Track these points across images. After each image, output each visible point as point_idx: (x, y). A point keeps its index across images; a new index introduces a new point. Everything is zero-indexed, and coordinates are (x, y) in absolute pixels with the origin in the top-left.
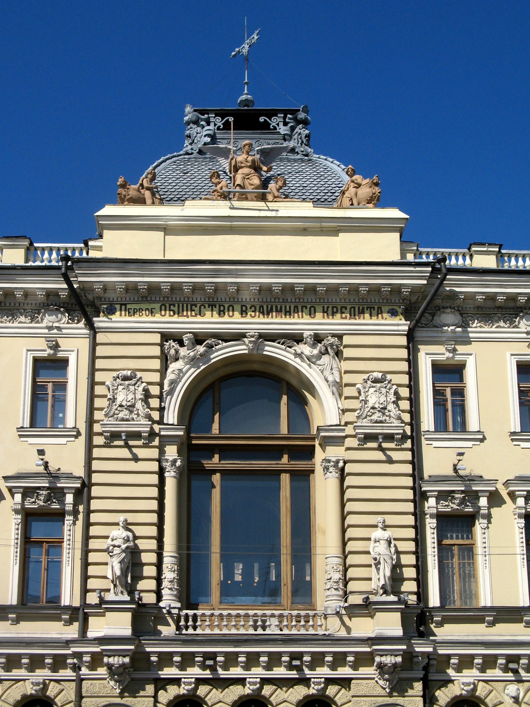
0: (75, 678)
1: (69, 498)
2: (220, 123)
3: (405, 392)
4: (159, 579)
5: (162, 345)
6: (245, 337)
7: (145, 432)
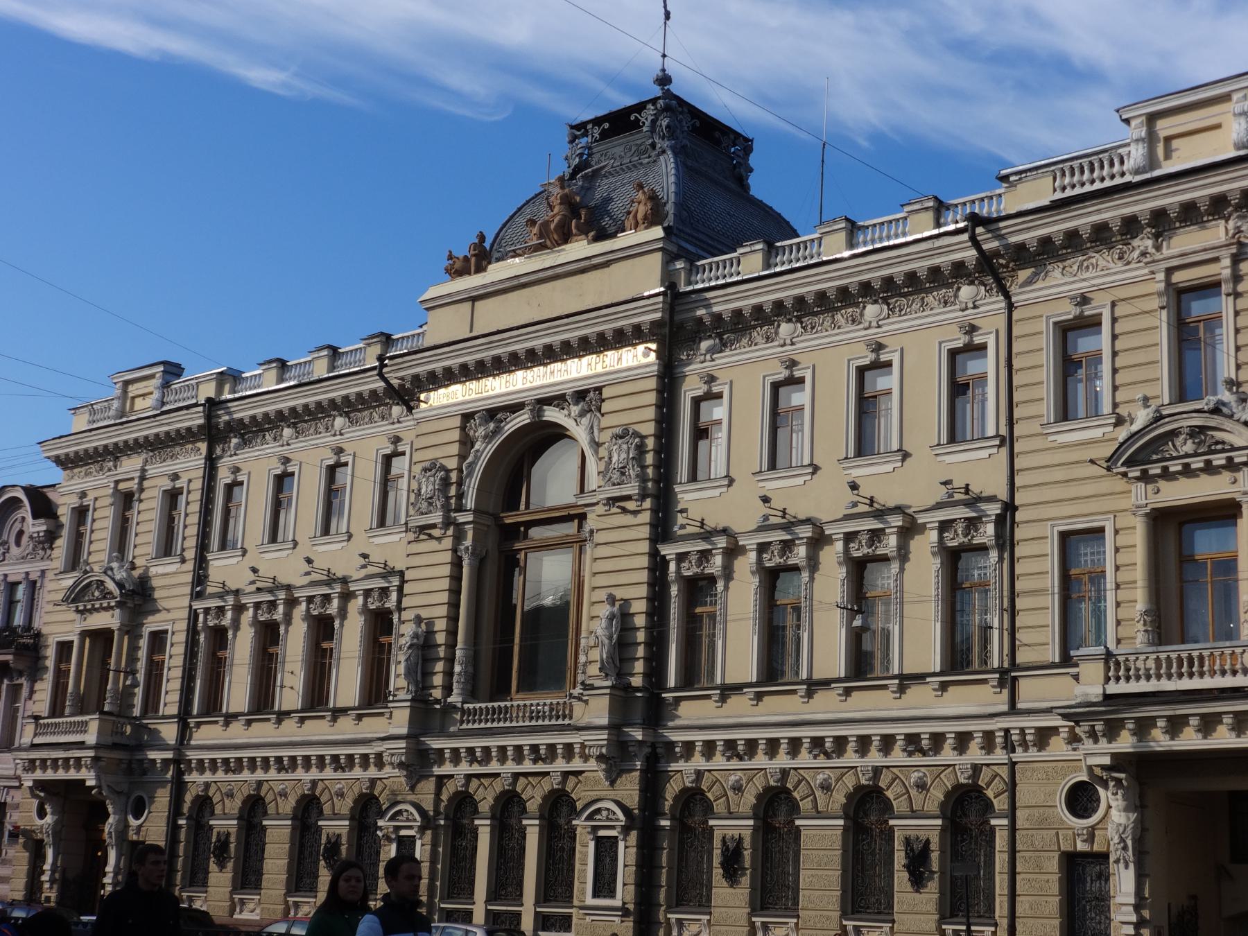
2: (596, 132)
3: (650, 443)
4: (449, 674)
5: (463, 428)
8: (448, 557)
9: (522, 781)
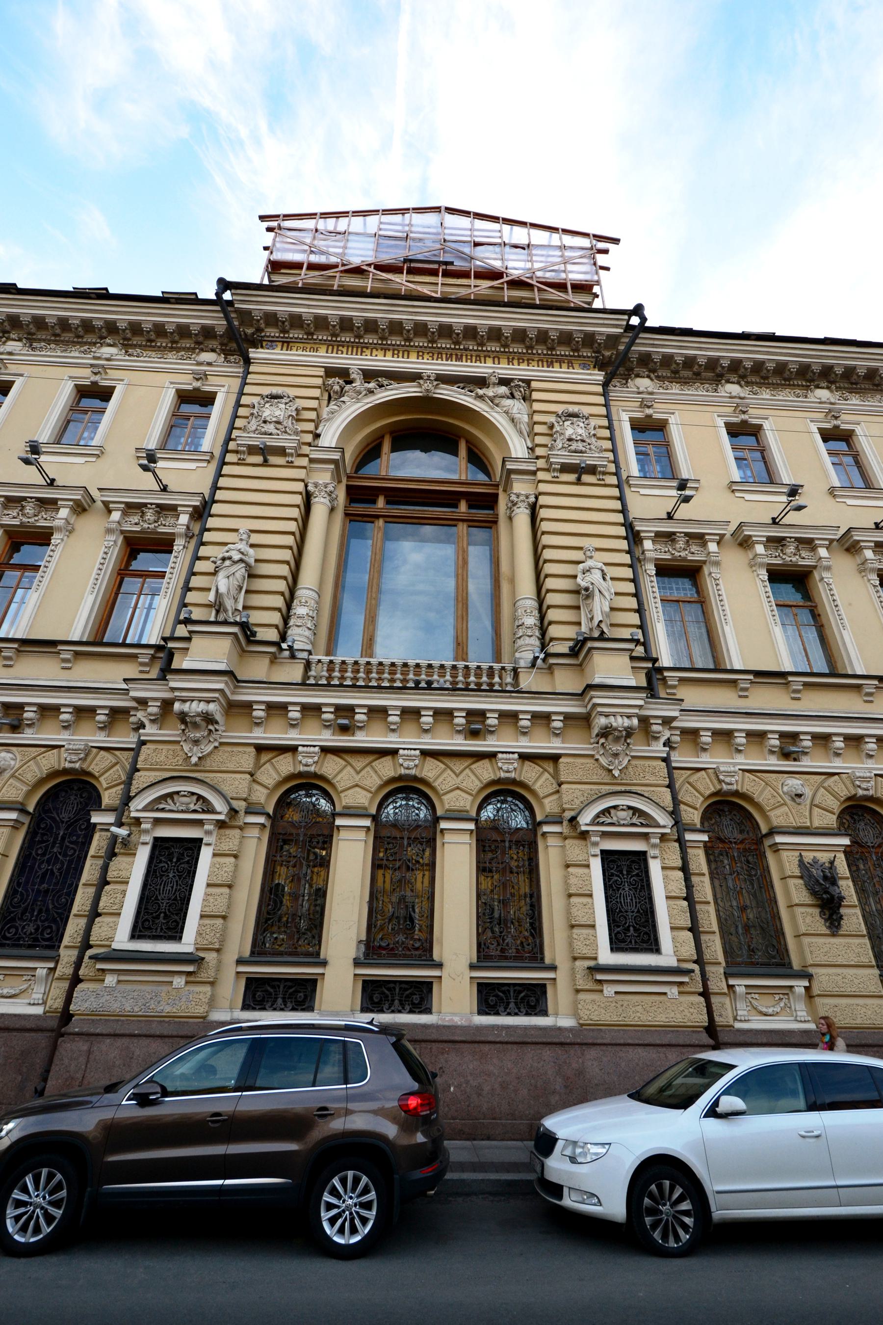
0: (134, 746)
1: (184, 519)
6: (421, 378)
7: (291, 448)
8: (300, 487)
9: (431, 762)
